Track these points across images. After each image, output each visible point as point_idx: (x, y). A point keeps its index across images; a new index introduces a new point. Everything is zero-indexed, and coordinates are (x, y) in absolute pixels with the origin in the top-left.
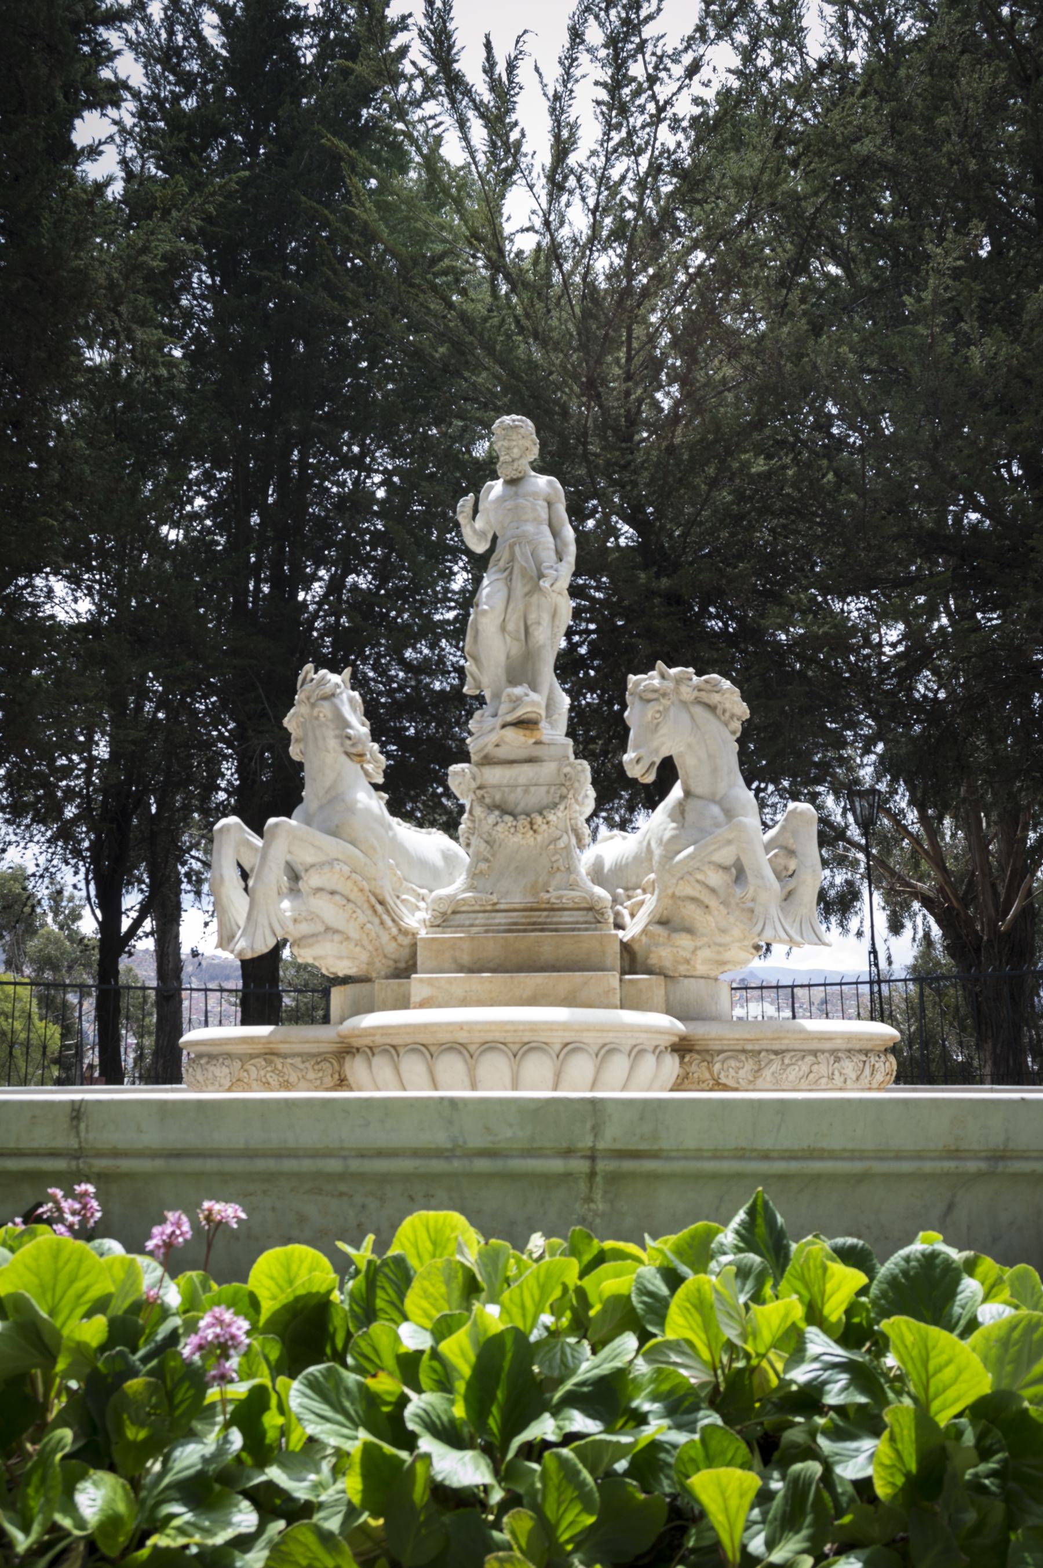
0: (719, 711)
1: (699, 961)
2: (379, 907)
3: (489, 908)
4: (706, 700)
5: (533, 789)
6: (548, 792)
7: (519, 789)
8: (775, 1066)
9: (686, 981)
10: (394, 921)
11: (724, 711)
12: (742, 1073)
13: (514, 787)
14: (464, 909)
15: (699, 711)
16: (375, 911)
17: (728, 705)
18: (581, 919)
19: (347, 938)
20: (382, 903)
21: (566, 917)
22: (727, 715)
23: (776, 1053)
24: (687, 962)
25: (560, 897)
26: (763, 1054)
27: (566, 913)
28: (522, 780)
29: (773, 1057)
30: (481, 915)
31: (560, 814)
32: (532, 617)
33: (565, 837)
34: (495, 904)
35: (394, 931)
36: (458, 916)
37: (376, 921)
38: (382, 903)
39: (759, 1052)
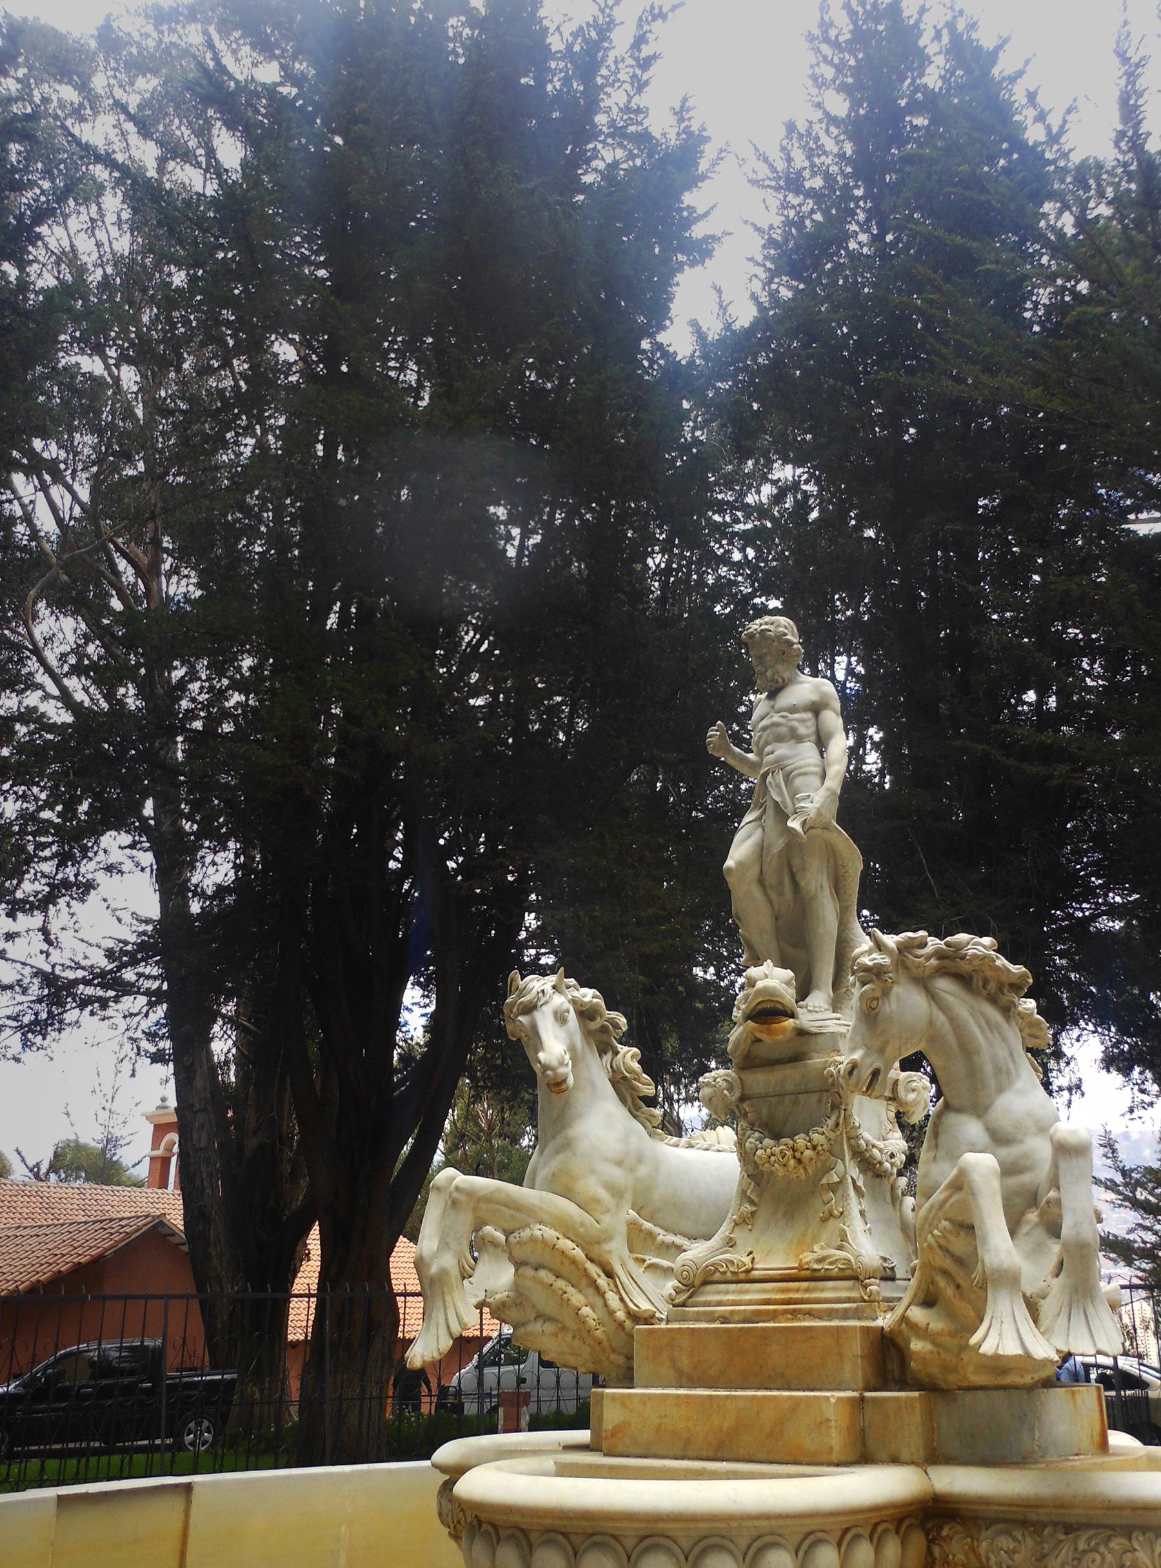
0: (977, 982)
1: (971, 1369)
2: (602, 1282)
3: (742, 1276)
4: (954, 970)
5: (802, 1098)
6: (820, 1101)
7: (787, 1099)
8: (1066, 1552)
9: (968, 1397)
10: (622, 1299)
11: (986, 982)
12: (1016, 1557)
13: (781, 1095)
14: (717, 1276)
15: (943, 985)
16: (597, 1289)
17: (988, 973)
18: (844, 1294)
19: (564, 1328)
20: (610, 1274)
21: (830, 1291)
22: (992, 986)
23: (1070, 1529)
24: (954, 1370)
25: (820, 1260)
26: (1048, 1531)
27: (830, 1284)
28: (790, 1087)
29: (1062, 1537)
30: (733, 1287)
31: (832, 1135)
32: (796, 862)
33: (840, 1166)
34: (748, 1271)
35: (621, 1315)
36: (709, 1288)
37: (599, 1302)
38: (610, 1274)
39: (1045, 1526)
